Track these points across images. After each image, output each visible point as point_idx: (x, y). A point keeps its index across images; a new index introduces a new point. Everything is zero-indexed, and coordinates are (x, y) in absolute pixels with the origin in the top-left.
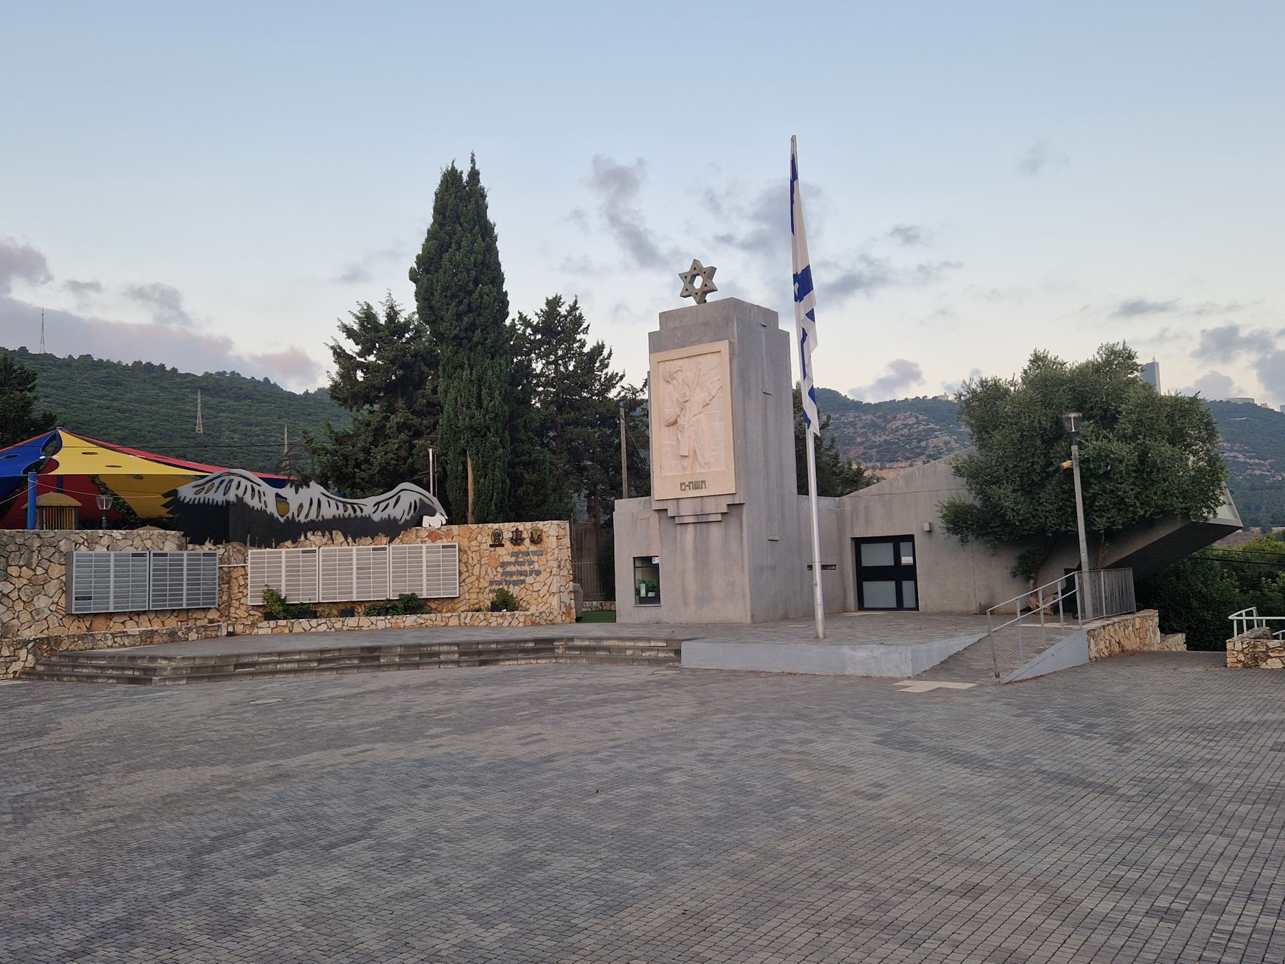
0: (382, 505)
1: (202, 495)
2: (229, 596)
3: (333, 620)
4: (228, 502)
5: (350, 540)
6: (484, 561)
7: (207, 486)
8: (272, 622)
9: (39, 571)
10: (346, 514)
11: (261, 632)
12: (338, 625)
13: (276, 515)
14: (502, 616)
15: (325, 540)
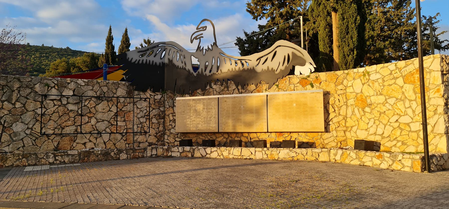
0: (263, 60)
1: (145, 58)
2: (164, 127)
3: (223, 148)
4: (163, 64)
5: (240, 87)
6: (351, 102)
7: (148, 52)
8: (180, 148)
9: (18, 105)
10: (237, 68)
11: (173, 154)
12: (225, 154)
13: (192, 71)
14: (378, 157)
15: (222, 88)
